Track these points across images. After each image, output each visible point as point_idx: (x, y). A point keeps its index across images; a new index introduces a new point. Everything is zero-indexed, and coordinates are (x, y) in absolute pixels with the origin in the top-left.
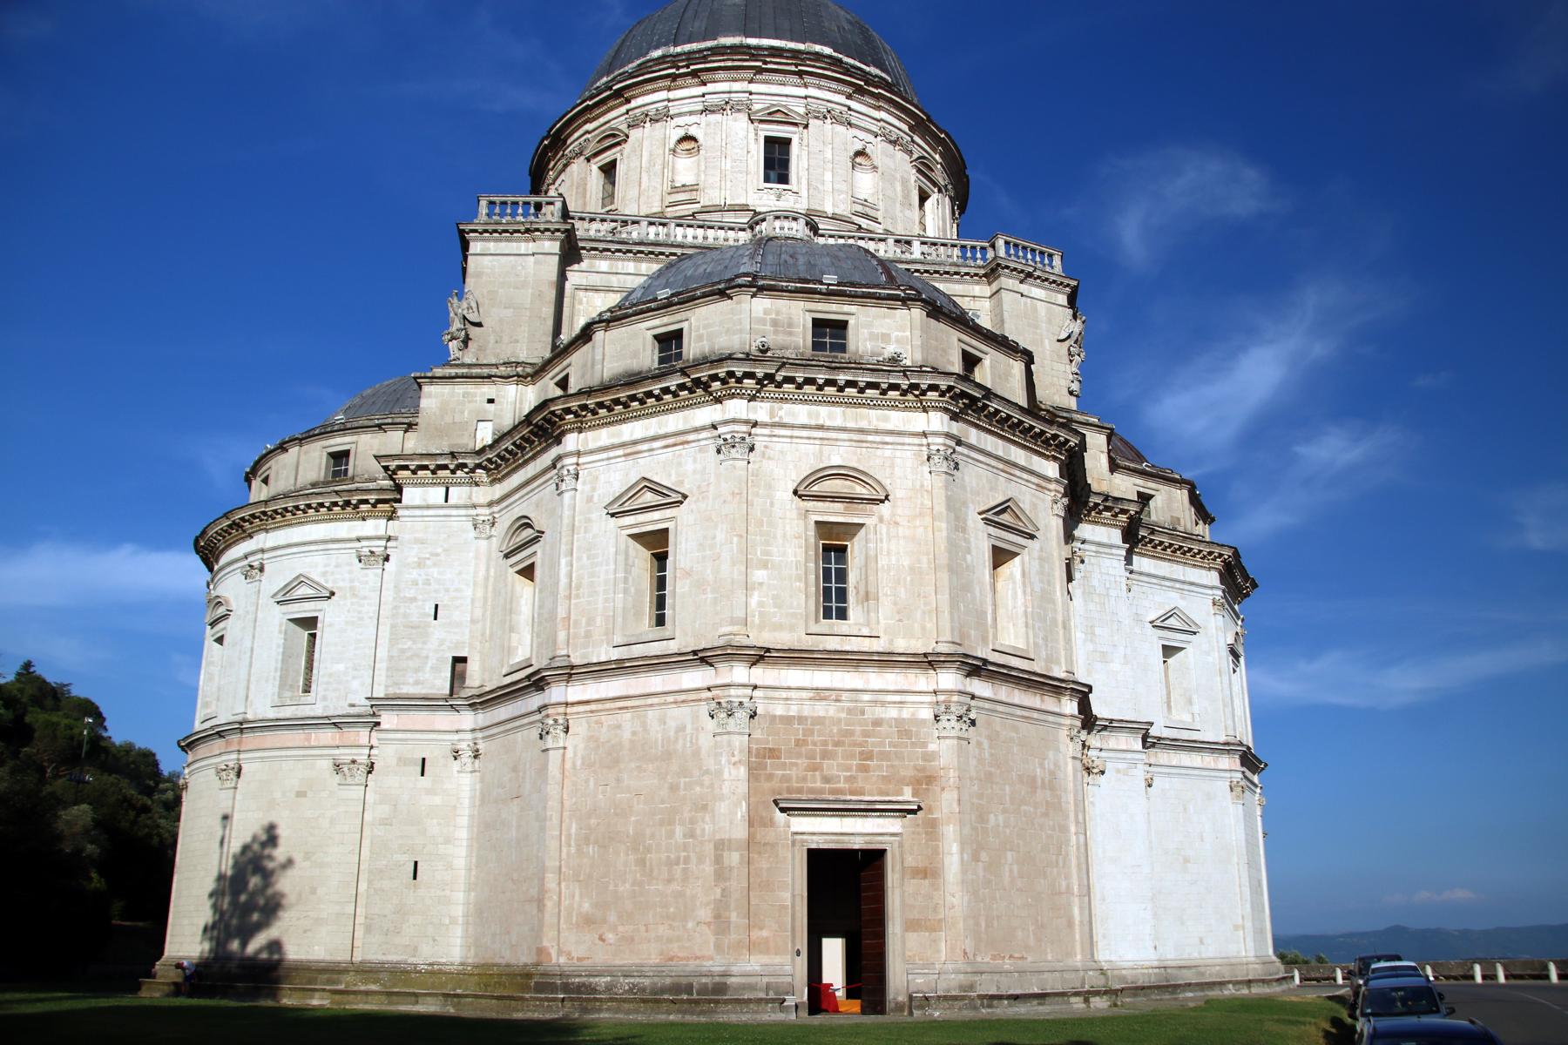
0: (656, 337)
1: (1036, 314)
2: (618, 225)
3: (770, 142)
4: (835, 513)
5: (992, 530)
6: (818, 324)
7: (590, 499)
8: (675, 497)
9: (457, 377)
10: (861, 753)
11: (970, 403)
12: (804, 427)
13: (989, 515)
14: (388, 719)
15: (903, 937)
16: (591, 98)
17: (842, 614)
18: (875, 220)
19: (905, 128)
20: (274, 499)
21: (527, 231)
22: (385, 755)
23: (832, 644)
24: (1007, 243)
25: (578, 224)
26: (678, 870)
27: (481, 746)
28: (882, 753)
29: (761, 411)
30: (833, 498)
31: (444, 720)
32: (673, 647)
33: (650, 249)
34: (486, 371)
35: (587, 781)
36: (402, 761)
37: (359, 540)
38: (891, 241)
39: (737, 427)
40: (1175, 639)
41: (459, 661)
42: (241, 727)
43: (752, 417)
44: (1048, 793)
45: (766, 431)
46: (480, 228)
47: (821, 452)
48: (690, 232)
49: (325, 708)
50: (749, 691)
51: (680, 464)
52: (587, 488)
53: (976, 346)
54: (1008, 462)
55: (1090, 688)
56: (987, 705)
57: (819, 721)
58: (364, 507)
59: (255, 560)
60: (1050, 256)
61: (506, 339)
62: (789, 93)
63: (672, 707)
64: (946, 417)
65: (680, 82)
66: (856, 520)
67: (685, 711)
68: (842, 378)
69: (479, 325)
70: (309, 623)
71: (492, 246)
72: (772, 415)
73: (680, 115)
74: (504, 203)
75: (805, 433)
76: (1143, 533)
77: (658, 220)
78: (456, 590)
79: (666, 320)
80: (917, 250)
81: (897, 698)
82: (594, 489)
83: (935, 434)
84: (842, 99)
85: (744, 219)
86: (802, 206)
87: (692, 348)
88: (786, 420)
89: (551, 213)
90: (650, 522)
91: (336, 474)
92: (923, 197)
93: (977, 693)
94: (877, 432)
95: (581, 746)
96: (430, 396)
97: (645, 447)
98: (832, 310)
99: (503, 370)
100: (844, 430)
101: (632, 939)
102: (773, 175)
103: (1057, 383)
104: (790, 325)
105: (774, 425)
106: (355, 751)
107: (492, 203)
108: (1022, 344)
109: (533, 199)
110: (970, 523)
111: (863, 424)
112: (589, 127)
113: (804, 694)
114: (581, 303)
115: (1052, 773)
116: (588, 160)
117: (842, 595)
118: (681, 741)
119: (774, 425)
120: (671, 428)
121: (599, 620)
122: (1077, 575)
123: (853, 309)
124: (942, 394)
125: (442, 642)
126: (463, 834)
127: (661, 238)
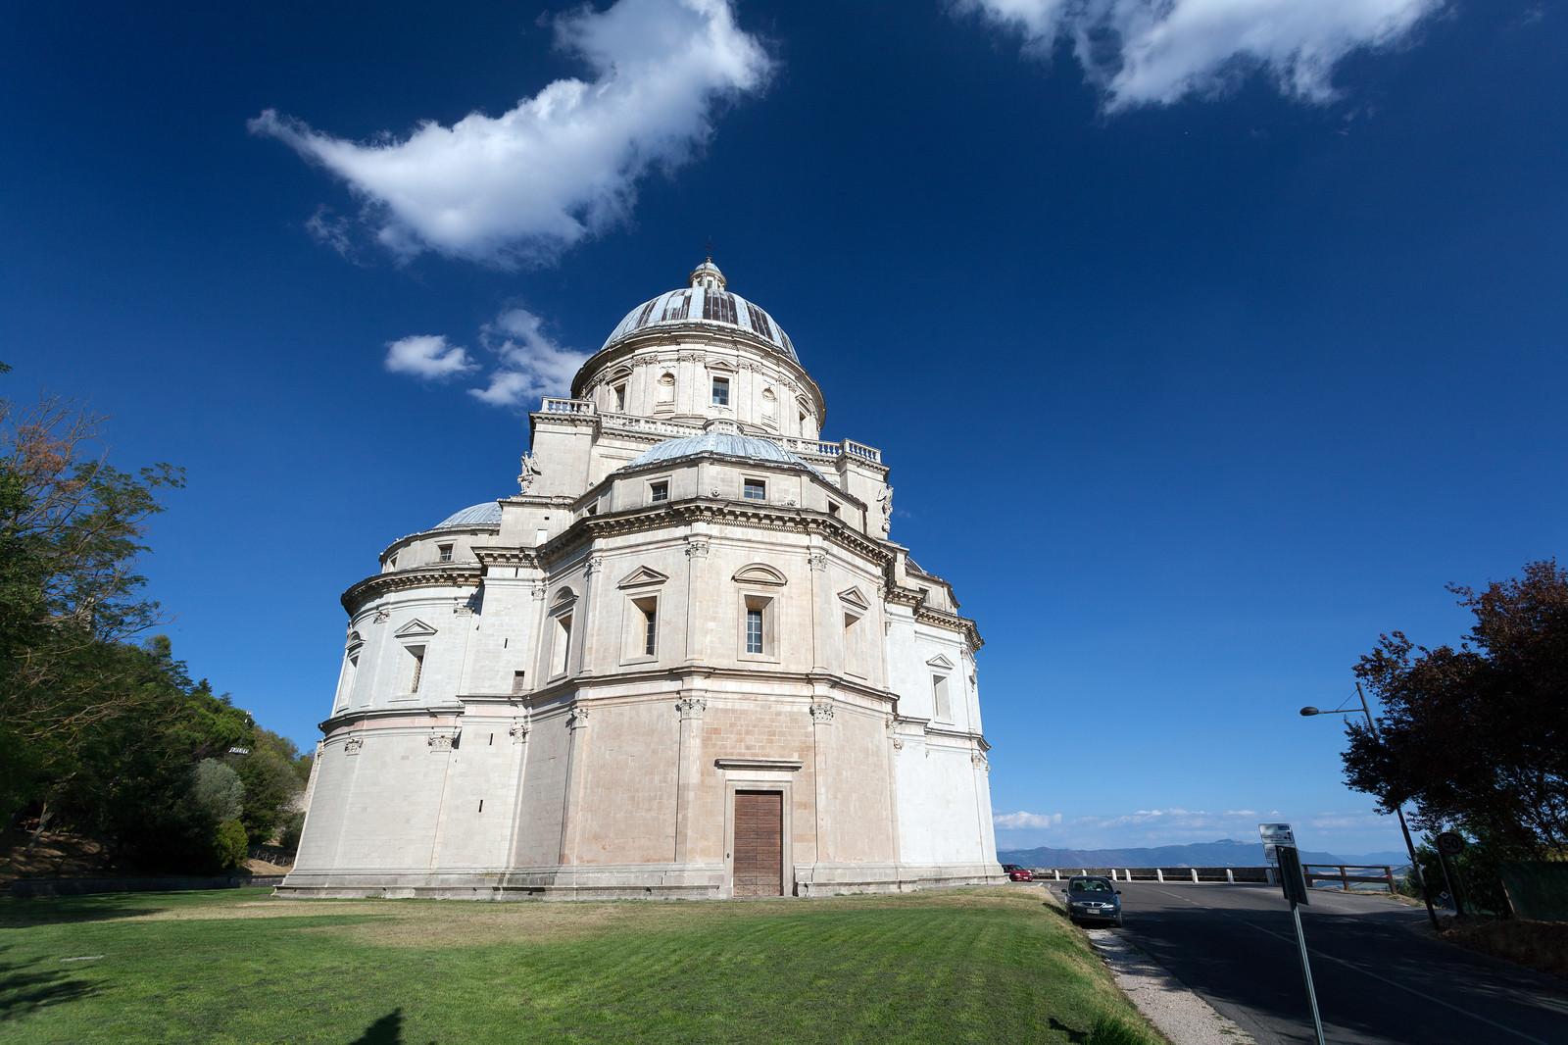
0: (651, 485)
1: (868, 484)
2: (627, 422)
3: (716, 380)
4: (757, 591)
5: (845, 604)
6: (748, 482)
7: (608, 578)
8: (661, 578)
9: (526, 503)
10: (769, 732)
11: (835, 531)
13: (843, 595)
14: (469, 709)
15: (792, 845)
17: (759, 650)
18: (775, 429)
19: (793, 378)
20: (401, 572)
22: (468, 731)
23: (754, 667)
24: (851, 445)
25: (603, 419)
26: (655, 804)
27: (530, 726)
28: (780, 732)
29: (714, 530)
30: (755, 582)
31: (507, 710)
32: (656, 667)
34: (544, 501)
35: (600, 748)
36: (477, 735)
37: (456, 599)
38: (785, 440)
39: (700, 538)
40: (940, 672)
41: (520, 674)
43: (709, 533)
44: (876, 759)
45: (717, 541)
46: (543, 416)
48: (669, 428)
50: (703, 693)
51: (665, 558)
52: (607, 571)
53: (837, 500)
54: (853, 566)
55: (899, 697)
56: (842, 705)
57: (744, 712)
60: (874, 453)
61: (557, 483)
63: (654, 702)
64: (821, 538)
67: (663, 704)
68: (762, 513)
69: (539, 473)
70: (418, 653)
71: (550, 427)
72: (721, 533)
73: (665, 361)
74: (559, 403)
75: (740, 544)
76: (922, 611)
77: (650, 421)
79: (658, 475)
80: (800, 447)
81: (790, 699)
83: (814, 547)
84: (758, 358)
85: (701, 423)
86: (735, 418)
87: (673, 494)
88: (728, 536)
89: (588, 412)
90: (646, 592)
91: (444, 558)
92: (802, 418)
93: (836, 698)
94: (781, 545)
97: (644, 548)
98: (757, 474)
99: (555, 501)
101: (624, 848)
103: (878, 525)
104: (732, 482)
105: (722, 538)
106: (444, 730)
107: (550, 402)
108: (862, 499)
109: (576, 402)
110: (833, 599)
111: (774, 541)
112: (609, 364)
113: (736, 696)
114: (603, 464)
115: (878, 747)
116: (608, 384)
117: (760, 638)
118: (660, 723)
119: (722, 538)
122: (888, 633)
123: (768, 474)
124: (818, 525)
126: (515, 782)
127: (653, 431)
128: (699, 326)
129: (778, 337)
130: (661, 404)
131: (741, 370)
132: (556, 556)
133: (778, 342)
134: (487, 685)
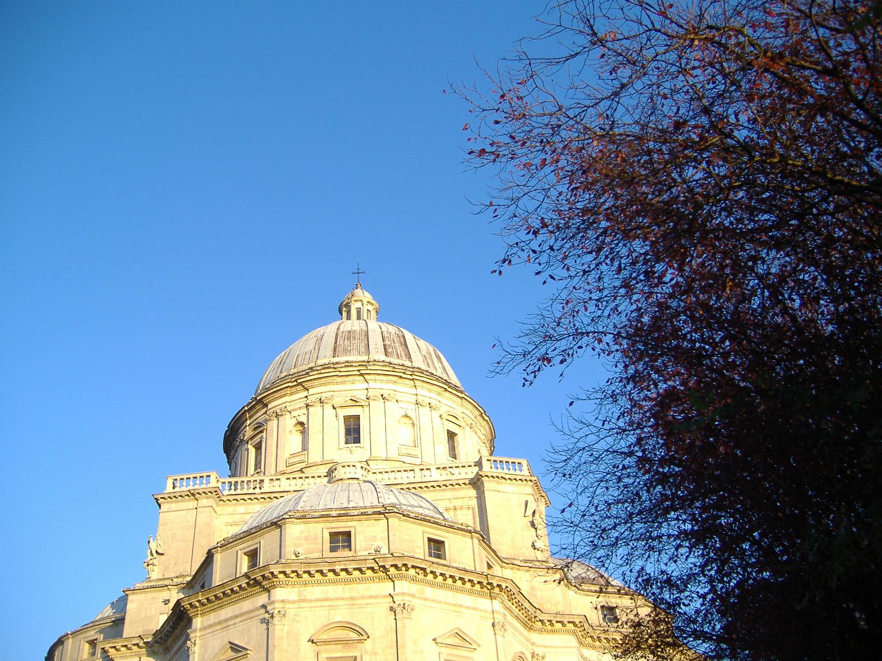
3: (347, 418)
5: (445, 651)
6: (334, 536)
12: (317, 600)
33: (268, 495)
38: (417, 469)
45: (296, 605)
47: (329, 614)
62: (356, 387)
66: (350, 654)
69: (163, 554)
71: (174, 506)
73: (295, 410)
79: (249, 543)
82: (206, 651)
88: (308, 597)
94: (362, 598)
96: (132, 601)
97: (232, 622)
98: (341, 526)
100: (342, 599)
102: (351, 438)
104: (316, 538)
111: (355, 594)
120: (245, 610)
128: (325, 367)
129: (420, 350)
130: (293, 455)
131: (371, 402)
132: (170, 640)
133: (418, 362)
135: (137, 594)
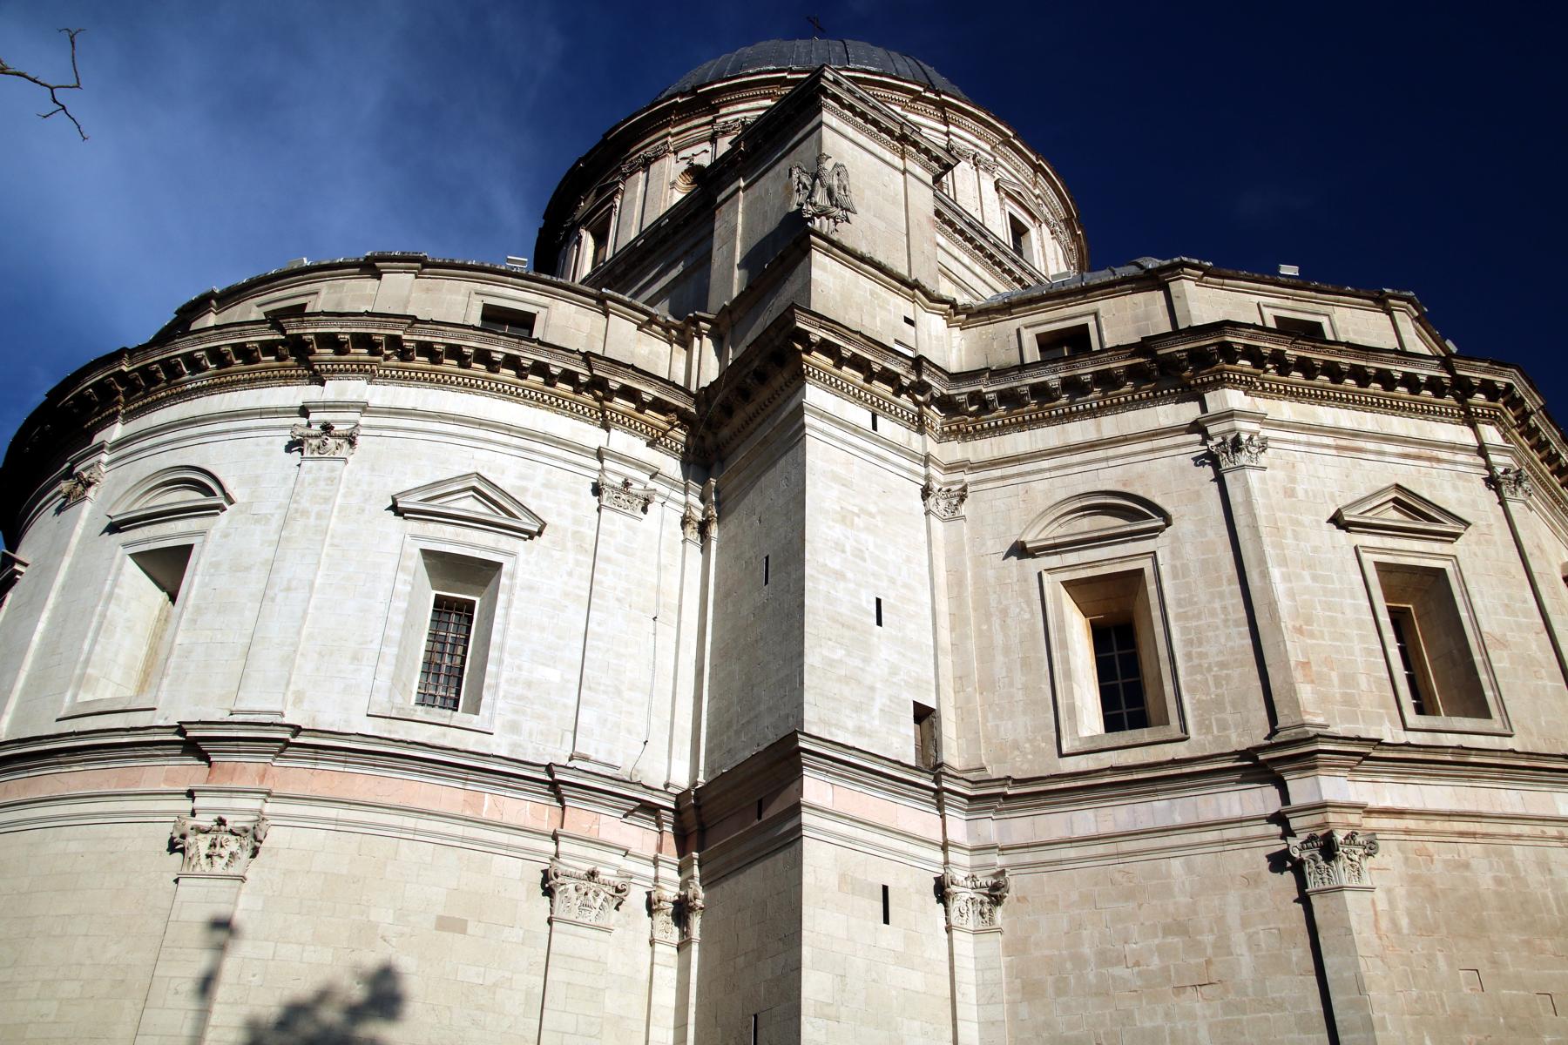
8: (1449, 527)
16: (791, 72)
21: (903, 139)
35: (1431, 959)
36: (849, 883)
42: (286, 742)
49: (515, 745)
58: (620, 403)
59: (342, 422)
65: (919, 105)
78: (906, 586)
79: (1289, 303)
95: (1400, 892)
97: (1371, 446)
106: (592, 852)
121: (1363, 681)
125: (894, 670)
134: (850, 724)
135: (834, 257)
